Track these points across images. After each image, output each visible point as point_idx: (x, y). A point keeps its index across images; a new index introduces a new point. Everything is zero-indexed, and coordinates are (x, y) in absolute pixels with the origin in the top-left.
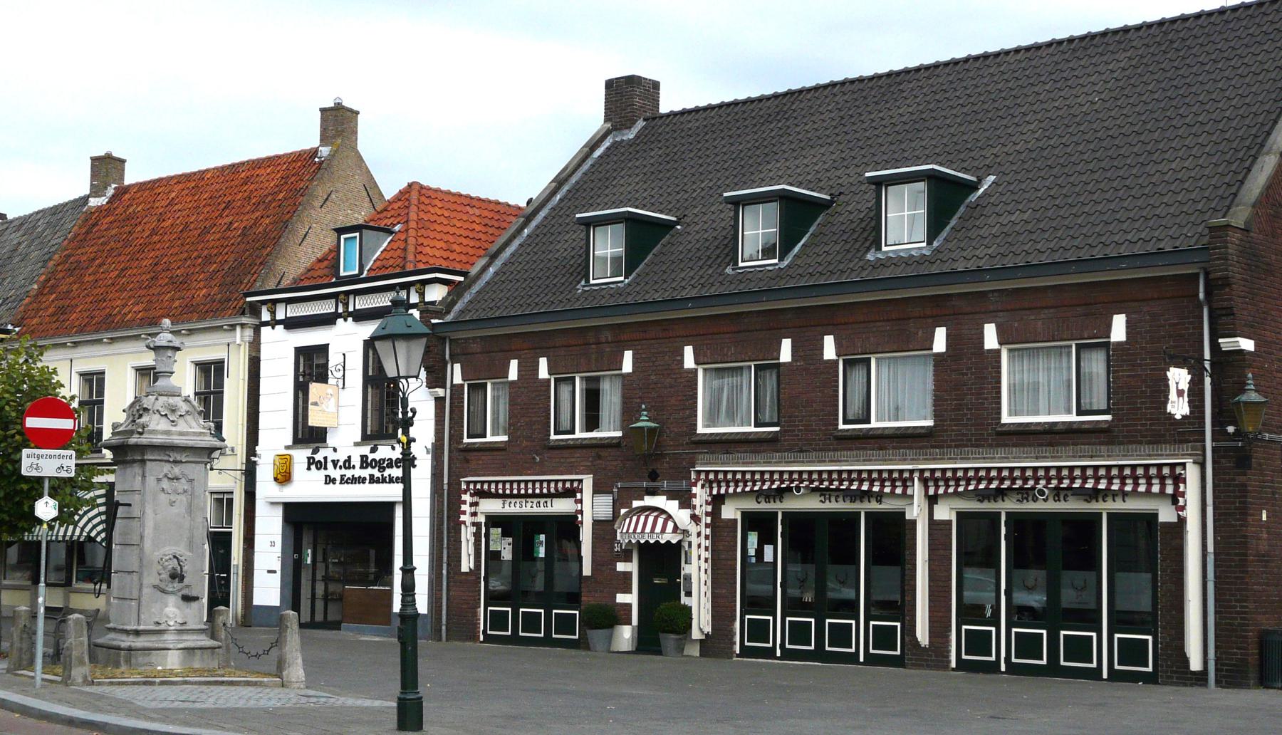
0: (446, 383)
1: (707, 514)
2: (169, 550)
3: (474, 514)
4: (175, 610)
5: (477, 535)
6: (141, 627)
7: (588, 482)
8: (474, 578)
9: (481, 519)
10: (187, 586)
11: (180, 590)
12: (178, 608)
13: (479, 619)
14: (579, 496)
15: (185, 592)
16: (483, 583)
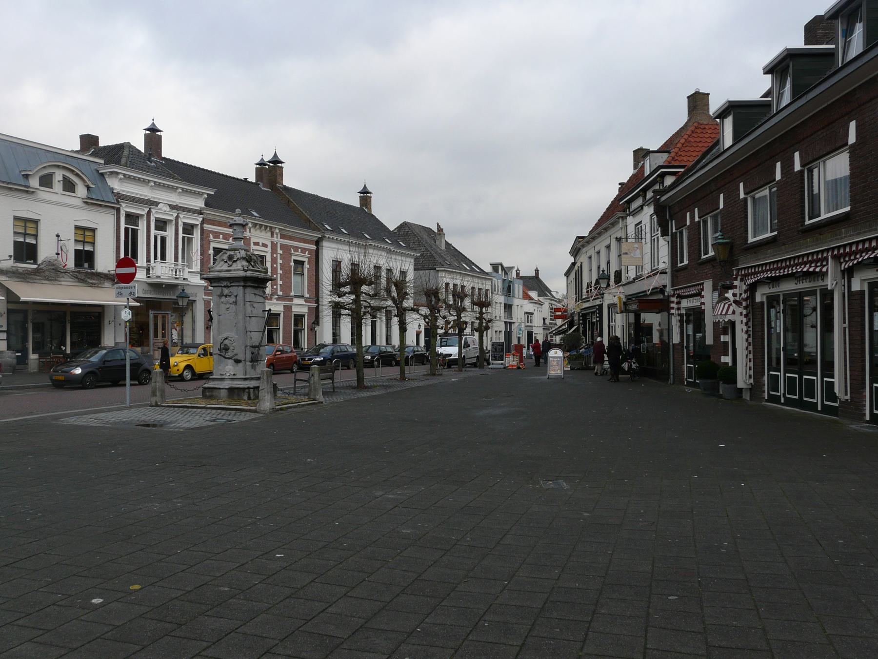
0: (668, 233)
1: (745, 300)
2: (225, 335)
3: (679, 309)
4: (231, 367)
5: (681, 321)
6: (247, 377)
7: (708, 285)
8: (680, 347)
9: (683, 312)
10: (236, 355)
11: (234, 356)
12: (233, 366)
13: (684, 372)
14: (703, 293)
15: (236, 357)
16: (685, 350)
